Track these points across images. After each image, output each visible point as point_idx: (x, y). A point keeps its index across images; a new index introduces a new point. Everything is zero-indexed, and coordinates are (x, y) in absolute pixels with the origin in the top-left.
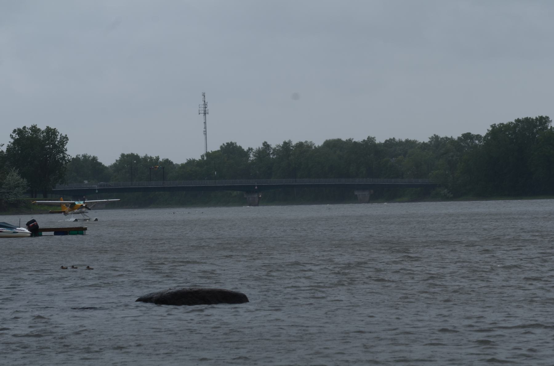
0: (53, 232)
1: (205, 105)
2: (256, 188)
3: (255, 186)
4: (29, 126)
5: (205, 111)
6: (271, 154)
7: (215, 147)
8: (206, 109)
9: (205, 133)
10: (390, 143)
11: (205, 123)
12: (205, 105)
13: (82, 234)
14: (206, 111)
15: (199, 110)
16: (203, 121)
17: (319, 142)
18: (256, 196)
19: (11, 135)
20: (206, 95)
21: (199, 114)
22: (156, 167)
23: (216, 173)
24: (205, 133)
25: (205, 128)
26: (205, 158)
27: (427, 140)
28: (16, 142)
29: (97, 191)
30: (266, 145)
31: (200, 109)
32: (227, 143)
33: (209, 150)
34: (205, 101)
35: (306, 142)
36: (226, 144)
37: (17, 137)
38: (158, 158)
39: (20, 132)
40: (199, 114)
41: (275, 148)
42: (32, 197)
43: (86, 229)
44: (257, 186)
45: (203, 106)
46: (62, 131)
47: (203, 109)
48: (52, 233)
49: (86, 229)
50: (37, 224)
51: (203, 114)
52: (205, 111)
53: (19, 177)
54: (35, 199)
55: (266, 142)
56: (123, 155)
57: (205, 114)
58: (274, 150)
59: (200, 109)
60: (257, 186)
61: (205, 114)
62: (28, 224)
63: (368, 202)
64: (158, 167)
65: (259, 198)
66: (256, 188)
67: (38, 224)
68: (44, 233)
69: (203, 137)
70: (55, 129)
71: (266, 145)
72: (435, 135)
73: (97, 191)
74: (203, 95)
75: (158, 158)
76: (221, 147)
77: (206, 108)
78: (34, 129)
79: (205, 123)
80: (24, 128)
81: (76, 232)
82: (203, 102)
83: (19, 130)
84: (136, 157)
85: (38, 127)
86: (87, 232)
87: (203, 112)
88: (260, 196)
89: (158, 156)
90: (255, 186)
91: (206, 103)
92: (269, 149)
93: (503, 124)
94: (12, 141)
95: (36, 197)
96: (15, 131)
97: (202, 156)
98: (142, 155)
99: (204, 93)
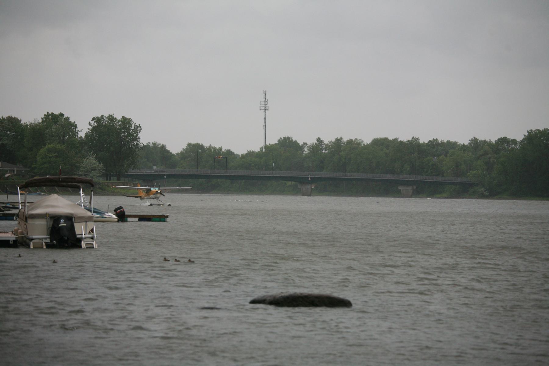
1: (266, 102)
3: (308, 178)
4: (106, 115)
5: (266, 107)
7: (273, 140)
8: (267, 106)
10: (434, 144)
11: (265, 118)
13: (164, 221)
14: (267, 107)
15: (260, 106)
16: (264, 117)
17: (367, 140)
18: (309, 187)
19: (89, 123)
20: (267, 93)
21: (260, 110)
22: (220, 157)
23: (273, 165)
25: (265, 123)
26: (264, 150)
27: (467, 142)
28: (94, 129)
29: (165, 177)
31: (262, 105)
33: (268, 143)
34: (265, 99)
35: (356, 139)
36: (283, 139)
37: (95, 124)
38: (221, 149)
39: (98, 120)
40: (260, 110)
41: (328, 144)
42: (107, 180)
43: (167, 217)
44: (311, 178)
45: (264, 103)
46: (136, 121)
48: (137, 219)
49: (167, 217)
50: (124, 210)
54: (110, 181)
55: (319, 138)
56: (189, 145)
57: (265, 110)
58: (327, 145)
59: (262, 105)
60: (311, 178)
61: (265, 110)
62: (115, 211)
63: (411, 197)
64: (221, 157)
65: (312, 188)
67: (125, 211)
68: (129, 219)
69: (263, 130)
70: (130, 118)
72: (474, 138)
73: (165, 177)
75: (221, 149)
76: (279, 141)
77: (266, 104)
78: (111, 118)
79: (265, 118)
80: (102, 116)
81: (159, 219)
83: (97, 118)
84: (202, 147)
85: (115, 116)
86: (168, 219)
87: (263, 108)
88: (313, 187)
89: (221, 147)
90: (308, 178)
91: (267, 101)
92: (322, 145)
93: (539, 130)
94: (90, 128)
95: (110, 180)
96: (93, 119)
97: (261, 149)
98: (206, 145)
99: (265, 91)
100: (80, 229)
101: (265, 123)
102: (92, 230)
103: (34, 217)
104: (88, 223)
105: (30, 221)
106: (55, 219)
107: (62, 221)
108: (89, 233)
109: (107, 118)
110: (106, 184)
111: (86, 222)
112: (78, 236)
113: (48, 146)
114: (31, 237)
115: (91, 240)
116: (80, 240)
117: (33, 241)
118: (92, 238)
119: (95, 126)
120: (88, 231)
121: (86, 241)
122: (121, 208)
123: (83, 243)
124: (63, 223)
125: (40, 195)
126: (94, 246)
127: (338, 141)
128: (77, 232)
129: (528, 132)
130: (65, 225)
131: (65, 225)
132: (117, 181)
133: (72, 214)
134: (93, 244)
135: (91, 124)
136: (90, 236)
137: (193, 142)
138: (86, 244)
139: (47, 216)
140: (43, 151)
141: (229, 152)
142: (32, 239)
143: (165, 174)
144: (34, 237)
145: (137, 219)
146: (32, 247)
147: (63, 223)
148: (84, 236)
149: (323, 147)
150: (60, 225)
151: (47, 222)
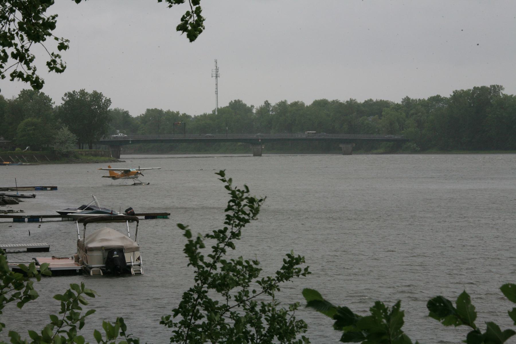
0: (144, 216)
1: (217, 70)
2: (260, 141)
3: (259, 139)
4: (78, 90)
5: (217, 75)
6: (271, 111)
7: (224, 103)
10: (369, 104)
11: (217, 84)
12: (217, 70)
13: (167, 218)
17: (308, 102)
20: (218, 62)
21: (212, 77)
22: (179, 123)
25: (217, 89)
26: (216, 113)
28: (67, 103)
29: (130, 142)
30: (267, 104)
31: (213, 73)
32: (235, 101)
33: (219, 107)
34: (216, 67)
36: (233, 101)
39: (70, 95)
40: (212, 77)
42: (80, 148)
43: (169, 214)
44: (261, 139)
47: (215, 73)
48: (143, 217)
49: (169, 214)
51: (215, 77)
52: (217, 75)
53: (69, 132)
54: (83, 150)
55: (267, 101)
58: (274, 107)
59: (213, 73)
60: (261, 139)
61: (217, 77)
63: (351, 154)
64: (180, 122)
65: (262, 149)
66: (260, 141)
69: (215, 95)
71: (267, 104)
73: (130, 142)
74: (215, 61)
76: (230, 104)
77: (217, 72)
78: (83, 93)
79: (217, 84)
80: (74, 92)
81: (162, 217)
83: (69, 93)
84: (161, 112)
87: (215, 75)
88: (263, 148)
89: (179, 111)
92: (269, 107)
93: (463, 90)
94: (63, 102)
95: (82, 149)
96: (66, 95)
97: (214, 111)
98: (165, 110)
99: (216, 60)
100: (129, 258)
101: (217, 89)
102: (139, 259)
103: (92, 249)
104: (135, 252)
105: (89, 253)
106: (110, 250)
107: (115, 253)
108: (137, 260)
109: (79, 92)
110: (80, 152)
111: (134, 252)
112: (127, 264)
113: (26, 120)
114: (90, 266)
115: (138, 267)
116: (130, 267)
117: (93, 269)
118: (139, 265)
119: (68, 100)
120: (136, 259)
121: (135, 268)
122: (131, 209)
123: (132, 269)
124: (116, 255)
125: (21, 165)
126: (141, 272)
128: (127, 260)
129: (454, 92)
130: (118, 256)
131: (118, 256)
132: (89, 150)
133: (123, 246)
134: (140, 271)
135: (64, 98)
136: (138, 263)
137: (152, 107)
138: (135, 271)
139: (103, 249)
140: (22, 125)
141: (185, 116)
142: (92, 268)
143: (130, 140)
144: (93, 266)
145: (143, 217)
146: (91, 273)
147: (116, 255)
148: (133, 264)
149: (270, 109)
150: (114, 256)
151: (103, 253)
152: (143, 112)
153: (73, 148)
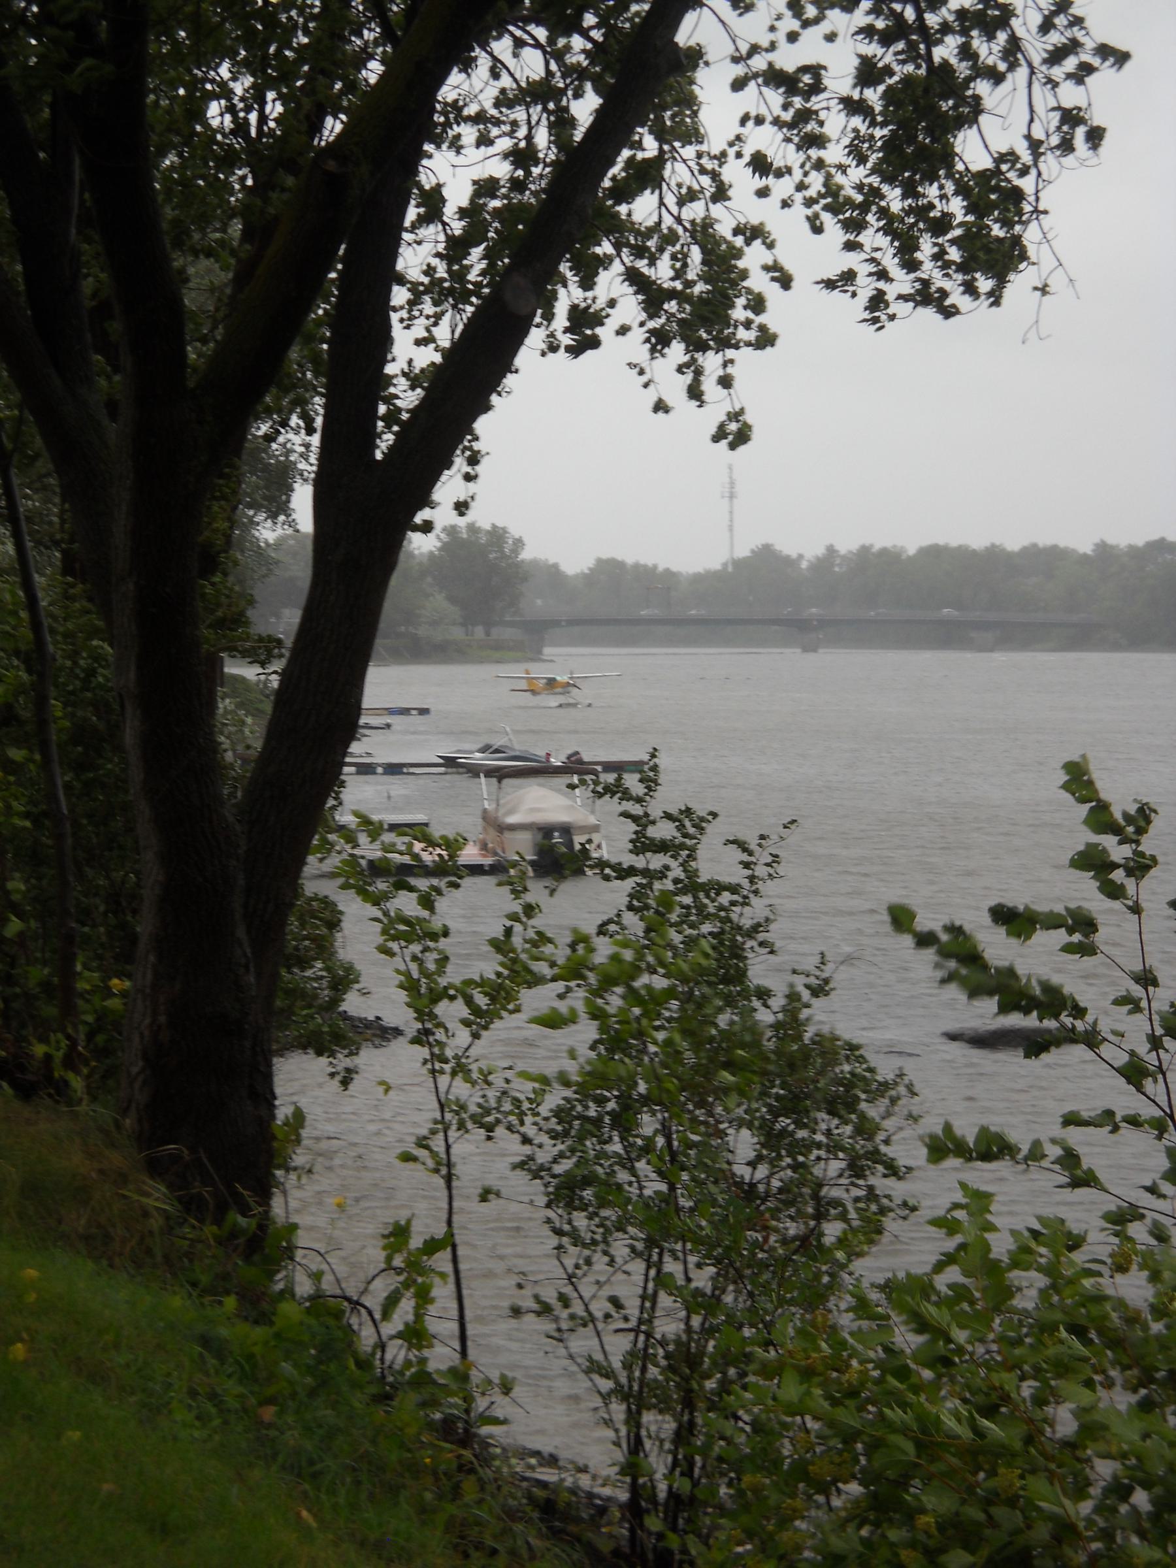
1: (732, 484)
9: (731, 528)
11: (731, 512)
12: (732, 484)
24: (731, 528)
26: (730, 569)
30: (831, 550)
35: (895, 546)
46: (515, 531)
55: (832, 546)
58: (844, 557)
63: (992, 650)
71: (831, 550)
79: (731, 512)
82: (727, 480)
94: (439, 544)
97: (725, 565)
98: (630, 560)
103: (513, 828)
105: (508, 835)
106: (546, 831)
107: (556, 834)
122: (577, 753)
124: (557, 838)
127: (865, 550)
137: (605, 556)
141: (668, 573)
147: (557, 838)
152: (591, 563)
153: (457, 633)
